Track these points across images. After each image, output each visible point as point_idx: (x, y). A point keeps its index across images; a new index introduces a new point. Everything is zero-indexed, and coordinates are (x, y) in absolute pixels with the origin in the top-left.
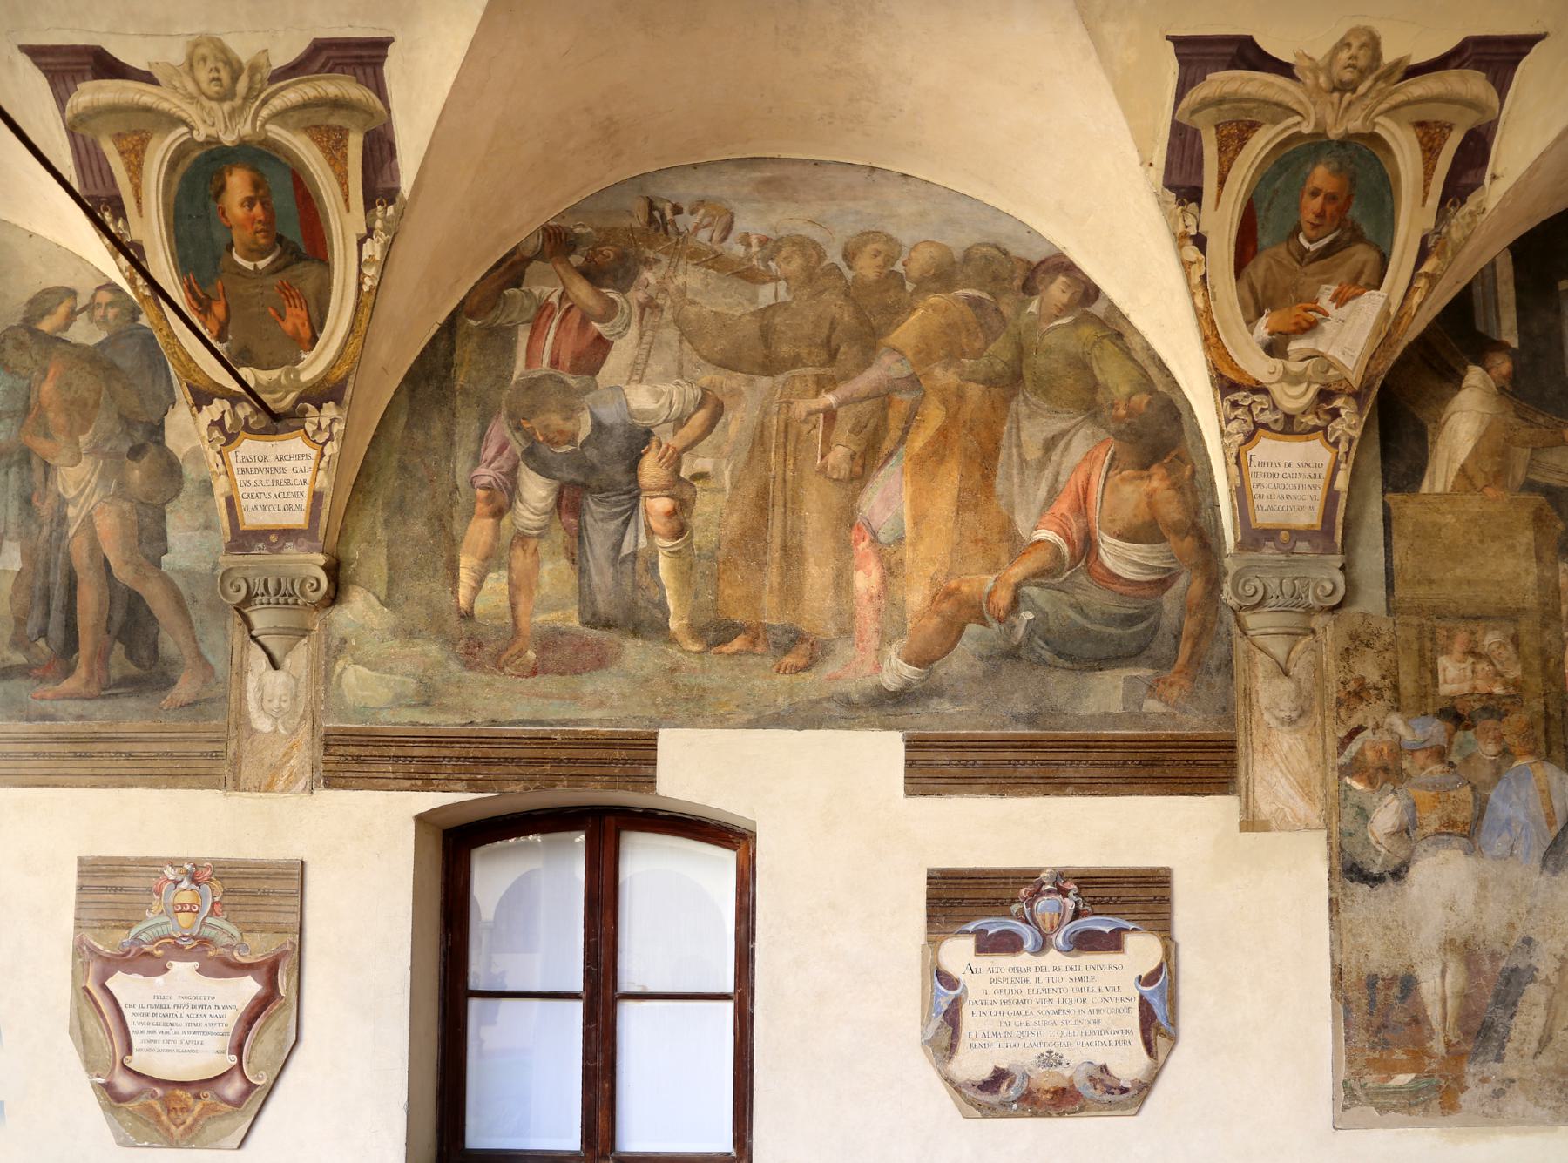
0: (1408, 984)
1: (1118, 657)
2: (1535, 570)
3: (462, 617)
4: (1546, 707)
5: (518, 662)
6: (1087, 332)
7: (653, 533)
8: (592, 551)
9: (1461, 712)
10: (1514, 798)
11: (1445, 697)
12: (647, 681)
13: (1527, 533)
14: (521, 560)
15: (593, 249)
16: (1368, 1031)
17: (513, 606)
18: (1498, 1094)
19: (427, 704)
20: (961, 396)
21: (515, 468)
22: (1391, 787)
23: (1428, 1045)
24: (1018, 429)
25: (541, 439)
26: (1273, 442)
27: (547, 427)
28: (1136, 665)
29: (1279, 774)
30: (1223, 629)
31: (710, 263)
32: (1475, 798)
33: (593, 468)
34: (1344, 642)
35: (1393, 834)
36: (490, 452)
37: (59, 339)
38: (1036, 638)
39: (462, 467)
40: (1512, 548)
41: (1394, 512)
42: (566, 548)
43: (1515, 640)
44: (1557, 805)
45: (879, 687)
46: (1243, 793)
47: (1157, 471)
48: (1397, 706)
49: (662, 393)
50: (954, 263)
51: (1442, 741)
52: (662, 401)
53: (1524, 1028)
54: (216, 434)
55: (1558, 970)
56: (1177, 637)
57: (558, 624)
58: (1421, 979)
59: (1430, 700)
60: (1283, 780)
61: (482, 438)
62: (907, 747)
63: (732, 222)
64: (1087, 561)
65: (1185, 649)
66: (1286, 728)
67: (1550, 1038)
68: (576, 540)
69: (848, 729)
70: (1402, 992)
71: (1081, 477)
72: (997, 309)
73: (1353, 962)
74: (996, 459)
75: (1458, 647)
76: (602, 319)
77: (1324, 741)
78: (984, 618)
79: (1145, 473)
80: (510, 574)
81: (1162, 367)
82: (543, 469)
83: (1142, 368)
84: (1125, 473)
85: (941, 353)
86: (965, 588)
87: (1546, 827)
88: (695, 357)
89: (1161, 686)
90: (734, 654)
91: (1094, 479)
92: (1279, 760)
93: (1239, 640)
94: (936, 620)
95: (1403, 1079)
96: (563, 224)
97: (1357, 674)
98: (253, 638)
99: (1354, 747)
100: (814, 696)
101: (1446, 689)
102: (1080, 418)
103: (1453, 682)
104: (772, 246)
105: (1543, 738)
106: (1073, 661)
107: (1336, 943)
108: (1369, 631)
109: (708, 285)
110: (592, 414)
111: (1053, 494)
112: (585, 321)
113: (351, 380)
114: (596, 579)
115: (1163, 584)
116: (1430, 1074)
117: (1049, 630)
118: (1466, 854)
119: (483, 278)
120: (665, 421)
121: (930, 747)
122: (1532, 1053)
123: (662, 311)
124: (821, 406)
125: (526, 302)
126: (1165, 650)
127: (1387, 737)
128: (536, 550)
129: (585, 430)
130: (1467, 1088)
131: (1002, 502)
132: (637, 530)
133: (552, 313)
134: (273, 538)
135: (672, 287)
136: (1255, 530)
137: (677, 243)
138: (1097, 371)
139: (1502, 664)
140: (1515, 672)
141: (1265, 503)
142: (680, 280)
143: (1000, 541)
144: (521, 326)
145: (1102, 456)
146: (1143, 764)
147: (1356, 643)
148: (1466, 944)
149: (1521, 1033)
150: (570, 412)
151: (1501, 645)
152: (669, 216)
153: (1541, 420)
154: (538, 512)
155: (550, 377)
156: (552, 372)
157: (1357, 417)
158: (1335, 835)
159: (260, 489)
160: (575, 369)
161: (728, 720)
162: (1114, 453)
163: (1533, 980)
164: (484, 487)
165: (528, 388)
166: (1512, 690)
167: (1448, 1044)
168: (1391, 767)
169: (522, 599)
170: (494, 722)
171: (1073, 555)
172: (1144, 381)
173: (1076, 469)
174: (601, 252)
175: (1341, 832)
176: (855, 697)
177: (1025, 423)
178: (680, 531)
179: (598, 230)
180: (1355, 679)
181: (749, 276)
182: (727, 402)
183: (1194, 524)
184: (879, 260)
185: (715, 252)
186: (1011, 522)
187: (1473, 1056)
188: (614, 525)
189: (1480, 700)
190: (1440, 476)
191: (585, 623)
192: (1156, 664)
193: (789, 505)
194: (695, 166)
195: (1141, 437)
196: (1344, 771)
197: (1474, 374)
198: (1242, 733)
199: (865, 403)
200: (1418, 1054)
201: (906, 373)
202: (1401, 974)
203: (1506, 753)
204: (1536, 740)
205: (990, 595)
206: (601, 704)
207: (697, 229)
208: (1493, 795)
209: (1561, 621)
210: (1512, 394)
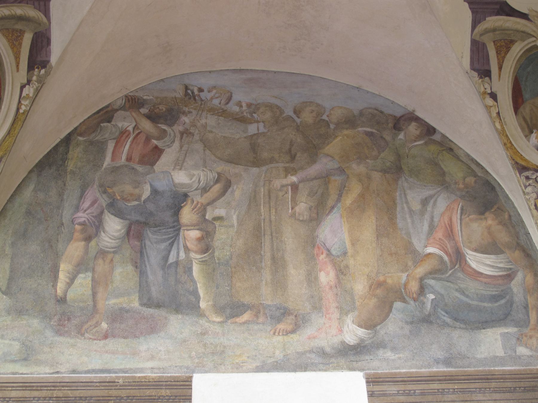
1: (493, 321)
3: (58, 301)
5: (94, 330)
6: (433, 148)
7: (189, 250)
8: (149, 261)
12: (185, 341)
14: (101, 266)
15: (154, 106)
17: (94, 294)
19: (25, 359)
20: (369, 178)
21: (102, 213)
24: (405, 194)
25: (119, 198)
27: (123, 191)
28: (505, 325)
31: (219, 114)
33: (151, 214)
36: (87, 204)
38: (439, 310)
39: (67, 214)
42: (132, 259)
45: (343, 343)
49: (194, 175)
50: (354, 116)
52: (193, 180)
56: (526, 307)
57: (125, 305)
61: (82, 196)
62: (367, 382)
63: (231, 96)
64: (460, 265)
68: (139, 255)
69: (325, 370)
71: (446, 219)
72: (382, 137)
74: (395, 209)
76: (158, 139)
78: (404, 299)
79: (483, 217)
80: (93, 274)
81: (478, 165)
82: (119, 214)
83: (467, 165)
85: (355, 157)
86: (389, 281)
88: (213, 157)
89: (525, 338)
90: (244, 323)
94: (374, 301)
96: (136, 94)
100: (300, 349)
104: (254, 107)
106: (465, 323)
109: (219, 124)
110: (151, 185)
111: (432, 228)
112: (148, 139)
113: (3, 160)
114: (151, 277)
115: (509, 276)
117: (446, 305)
119: (89, 118)
120: (196, 189)
121: (383, 382)
123: (193, 135)
124: (289, 183)
125: (114, 130)
128: (112, 260)
129: (146, 193)
131: (404, 232)
132: (178, 249)
133: (130, 133)
135: (199, 124)
137: (201, 105)
138: (443, 166)
142: (203, 121)
143: (406, 254)
144: (110, 141)
145: (456, 208)
150: (137, 184)
152: (196, 92)
154: (115, 238)
155: (126, 166)
156: (127, 163)
160: (142, 162)
161: (242, 367)
162: (462, 207)
164: (80, 224)
165: (112, 171)
169: (100, 290)
170: (74, 372)
171: (451, 261)
172: (470, 171)
173: (443, 214)
174: (158, 108)
176: (328, 350)
177: (408, 192)
178: (206, 249)
179: (157, 98)
181: (241, 120)
182: (233, 180)
184: (314, 114)
185: (222, 109)
186: (410, 243)
188: (163, 246)
191: (142, 305)
192: (517, 324)
193: (274, 234)
194: (210, 72)
195: (475, 198)
199: (314, 181)
201: (336, 166)
205: (406, 285)
206: (152, 358)
207: (212, 99)
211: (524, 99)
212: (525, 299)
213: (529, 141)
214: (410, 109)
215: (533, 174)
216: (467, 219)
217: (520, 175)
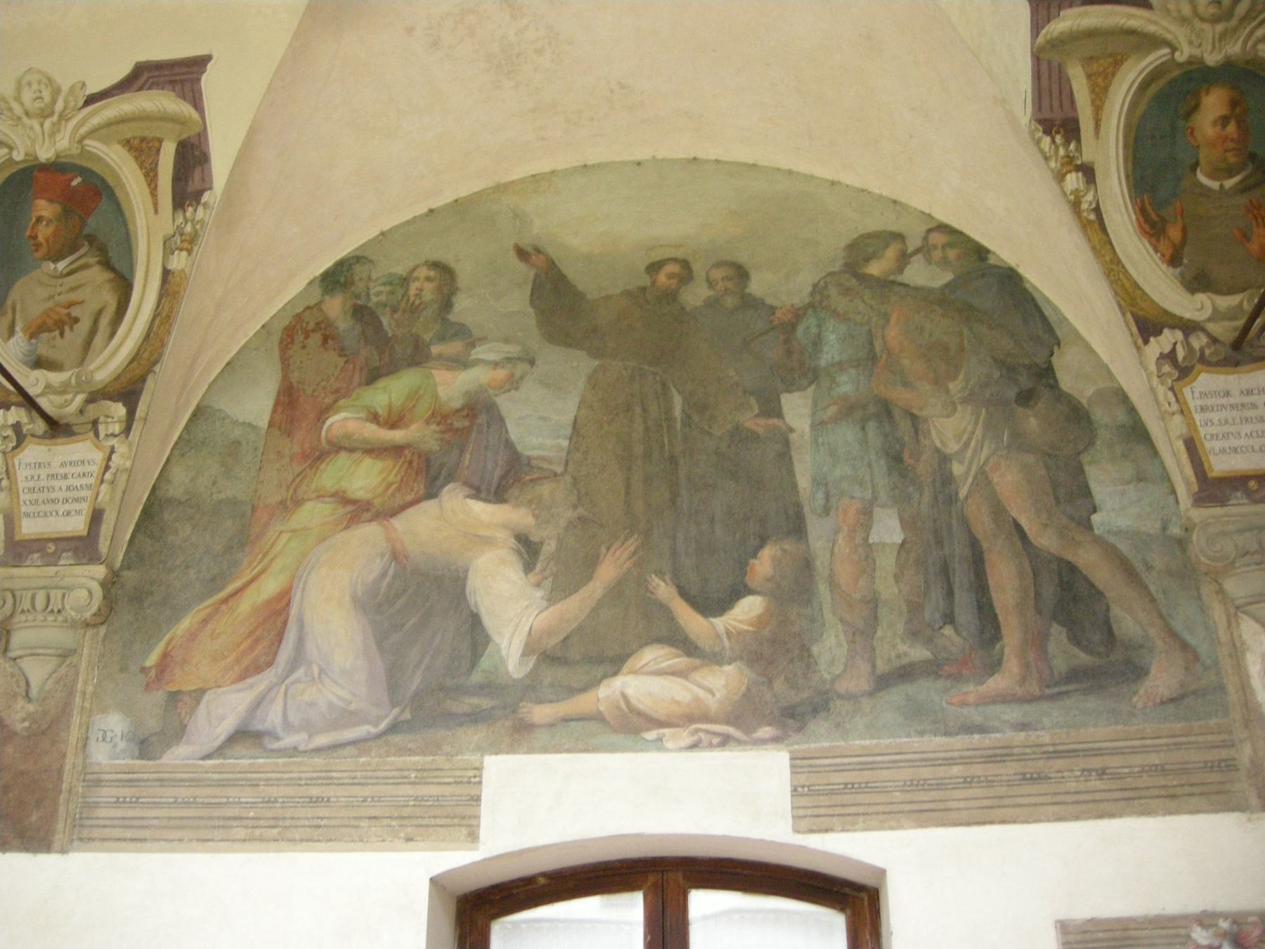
37: (893, 282)
54: (1167, 368)
98: (1237, 608)
134: (1252, 484)
159: (1226, 428)
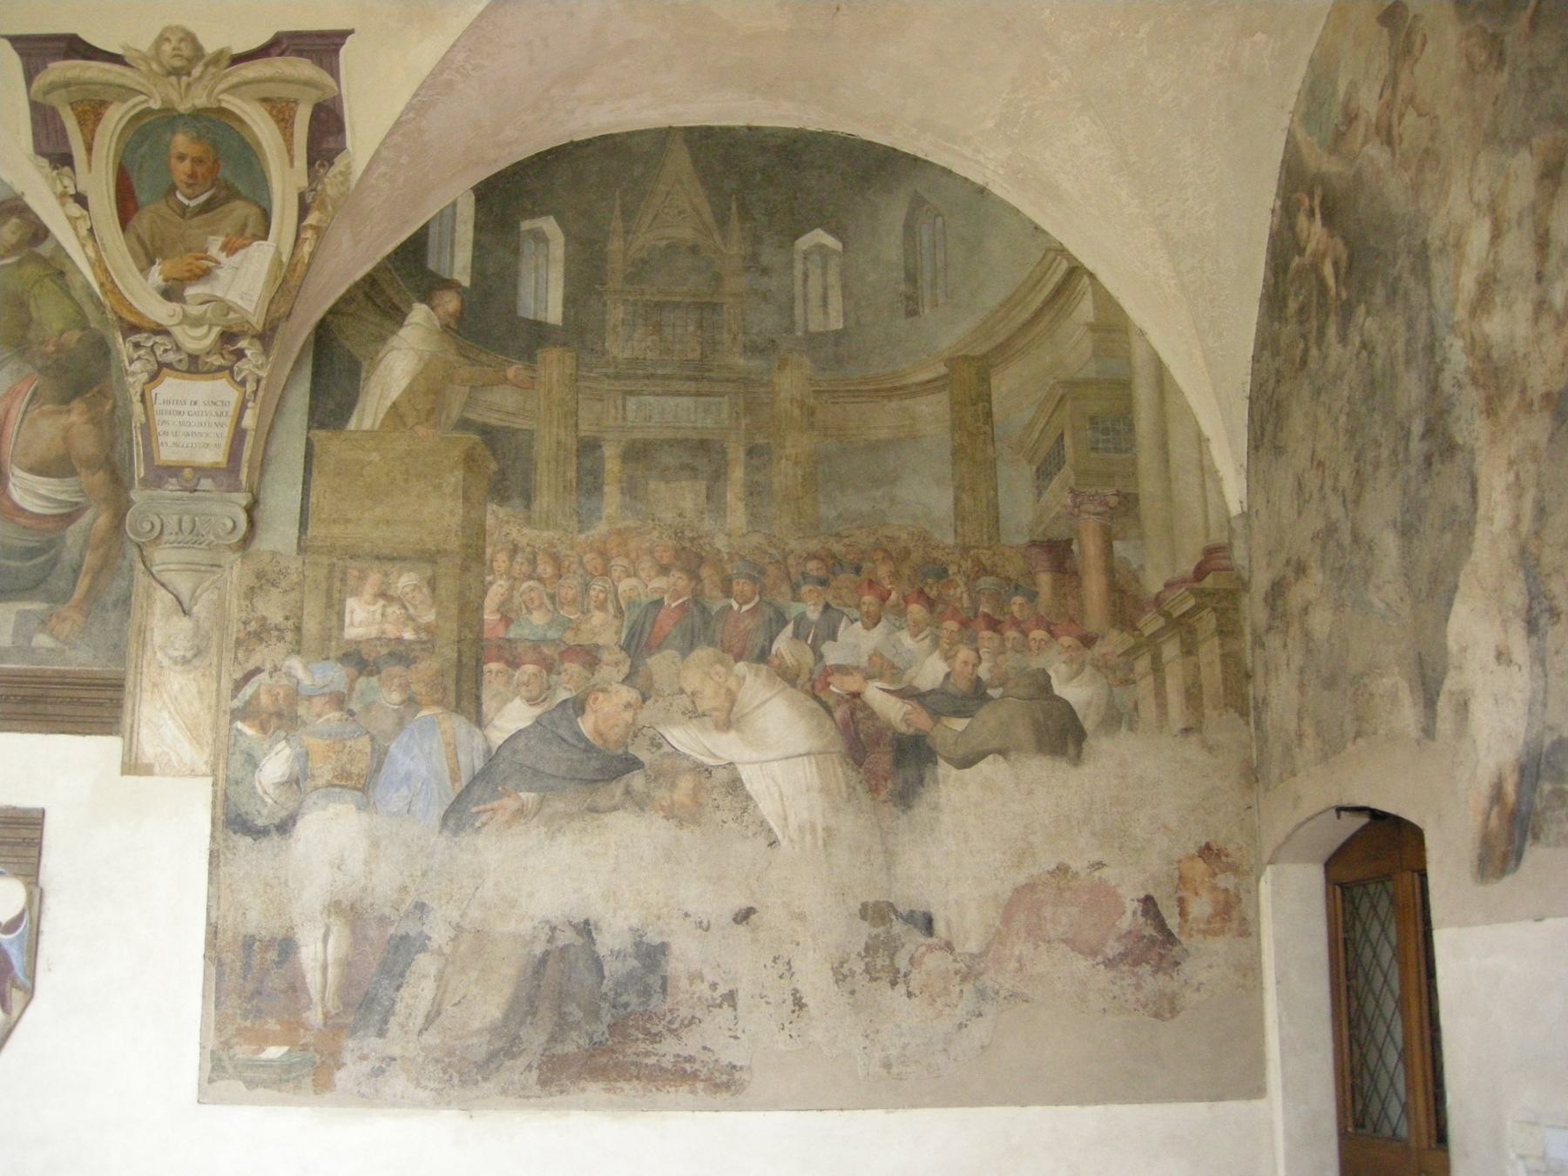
0: (286, 947)
2: (461, 511)
4: (460, 655)
6: (31, 270)
9: (365, 657)
10: (416, 751)
11: (348, 642)
13: (456, 473)
16: (240, 997)
18: (378, 1072)
22: (283, 734)
23: (304, 1015)
26: (177, 381)
28: (31, 599)
29: (165, 714)
30: (126, 563)
32: (373, 748)
34: (250, 580)
35: (283, 784)
40: (439, 486)
41: (317, 448)
43: (432, 583)
44: (462, 758)
46: (127, 735)
47: (77, 405)
48: (297, 649)
51: (343, 688)
53: (411, 1001)
55: (453, 940)
56: (76, 572)
58: (301, 943)
59: (333, 643)
60: (170, 722)
65: (83, 583)
66: (179, 668)
67: (439, 1013)
70: (279, 956)
73: (230, 919)
75: (369, 589)
77: (219, 683)
79: (64, 408)
83: (79, 305)
84: (45, 408)
87: (449, 782)
91: (13, 413)
92: (168, 701)
93: (141, 575)
95: (274, 1052)
97: (259, 614)
99: (248, 691)
101: (351, 633)
102: (7, 355)
103: (360, 624)
105: (453, 687)
107: (214, 900)
108: (277, 569)
115: (68, 518)
116: (305, 1048)
118: (359, 809)
122: (417, 1030)
126: (62, 584)
127: (284, 681)
130: (344, 1064)
136: (159, 467)
139: (416, 607)
140: (429, 617)
141: (170, 439)
146: (25, 700)
147: (262, 581)
148: (352, 907)
149: (407, 1006)
151: (416, 588)
153: (483, 358)
157: (264, 358)
158: (221, 782)
162: (36, 388)
163: (423, 948)
166: (423, 636)
167: (326, 1015)
168: (286, 713)
175: (227, 779)
180: (257, 619)
183: (108, 458)
187: (353, 1031)
189: (387, 645)
190: (369, 414)
192: (51, 598)
196: (236, 714)
197: (419, 313)
198: (132, 671)
200: (293, 1027)
202: (280, 937)
203: (412, 702)
204: (445, 689)
208: (394, 747)
209: (484, 564)
210: (457, 332)
211: (140, 204)
212: (81, 555)
213: (147, 280)
214: (18, 188)
215: (147, 338)
216: (37, 411)
217: (124, 339)
